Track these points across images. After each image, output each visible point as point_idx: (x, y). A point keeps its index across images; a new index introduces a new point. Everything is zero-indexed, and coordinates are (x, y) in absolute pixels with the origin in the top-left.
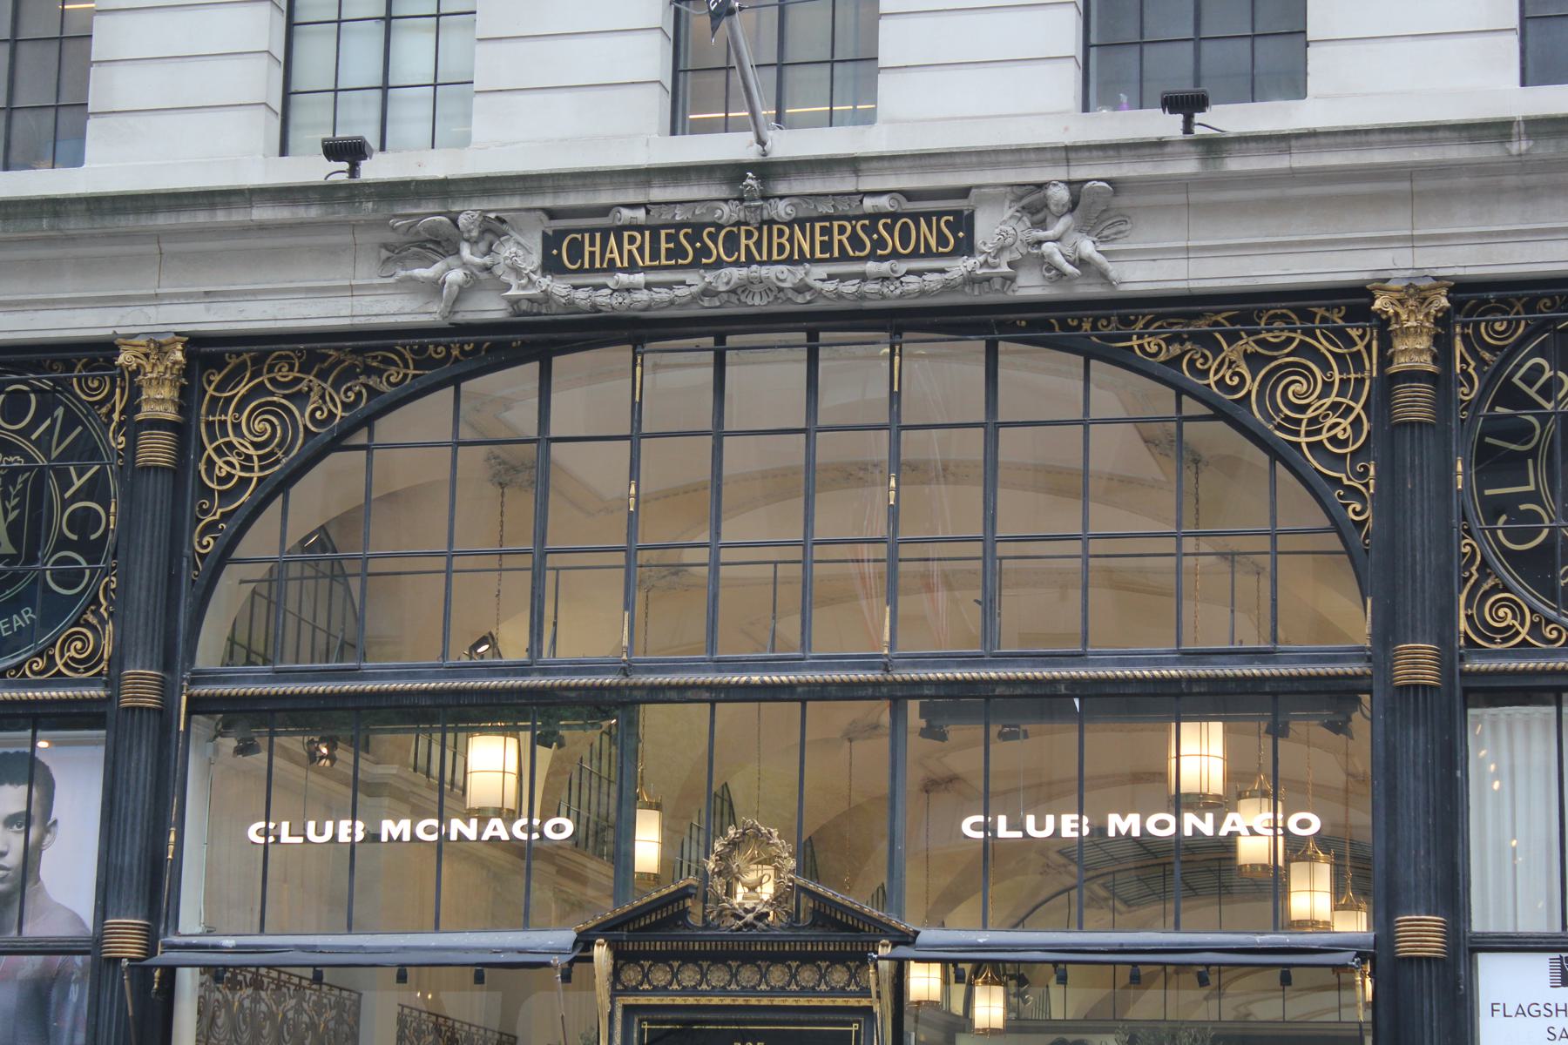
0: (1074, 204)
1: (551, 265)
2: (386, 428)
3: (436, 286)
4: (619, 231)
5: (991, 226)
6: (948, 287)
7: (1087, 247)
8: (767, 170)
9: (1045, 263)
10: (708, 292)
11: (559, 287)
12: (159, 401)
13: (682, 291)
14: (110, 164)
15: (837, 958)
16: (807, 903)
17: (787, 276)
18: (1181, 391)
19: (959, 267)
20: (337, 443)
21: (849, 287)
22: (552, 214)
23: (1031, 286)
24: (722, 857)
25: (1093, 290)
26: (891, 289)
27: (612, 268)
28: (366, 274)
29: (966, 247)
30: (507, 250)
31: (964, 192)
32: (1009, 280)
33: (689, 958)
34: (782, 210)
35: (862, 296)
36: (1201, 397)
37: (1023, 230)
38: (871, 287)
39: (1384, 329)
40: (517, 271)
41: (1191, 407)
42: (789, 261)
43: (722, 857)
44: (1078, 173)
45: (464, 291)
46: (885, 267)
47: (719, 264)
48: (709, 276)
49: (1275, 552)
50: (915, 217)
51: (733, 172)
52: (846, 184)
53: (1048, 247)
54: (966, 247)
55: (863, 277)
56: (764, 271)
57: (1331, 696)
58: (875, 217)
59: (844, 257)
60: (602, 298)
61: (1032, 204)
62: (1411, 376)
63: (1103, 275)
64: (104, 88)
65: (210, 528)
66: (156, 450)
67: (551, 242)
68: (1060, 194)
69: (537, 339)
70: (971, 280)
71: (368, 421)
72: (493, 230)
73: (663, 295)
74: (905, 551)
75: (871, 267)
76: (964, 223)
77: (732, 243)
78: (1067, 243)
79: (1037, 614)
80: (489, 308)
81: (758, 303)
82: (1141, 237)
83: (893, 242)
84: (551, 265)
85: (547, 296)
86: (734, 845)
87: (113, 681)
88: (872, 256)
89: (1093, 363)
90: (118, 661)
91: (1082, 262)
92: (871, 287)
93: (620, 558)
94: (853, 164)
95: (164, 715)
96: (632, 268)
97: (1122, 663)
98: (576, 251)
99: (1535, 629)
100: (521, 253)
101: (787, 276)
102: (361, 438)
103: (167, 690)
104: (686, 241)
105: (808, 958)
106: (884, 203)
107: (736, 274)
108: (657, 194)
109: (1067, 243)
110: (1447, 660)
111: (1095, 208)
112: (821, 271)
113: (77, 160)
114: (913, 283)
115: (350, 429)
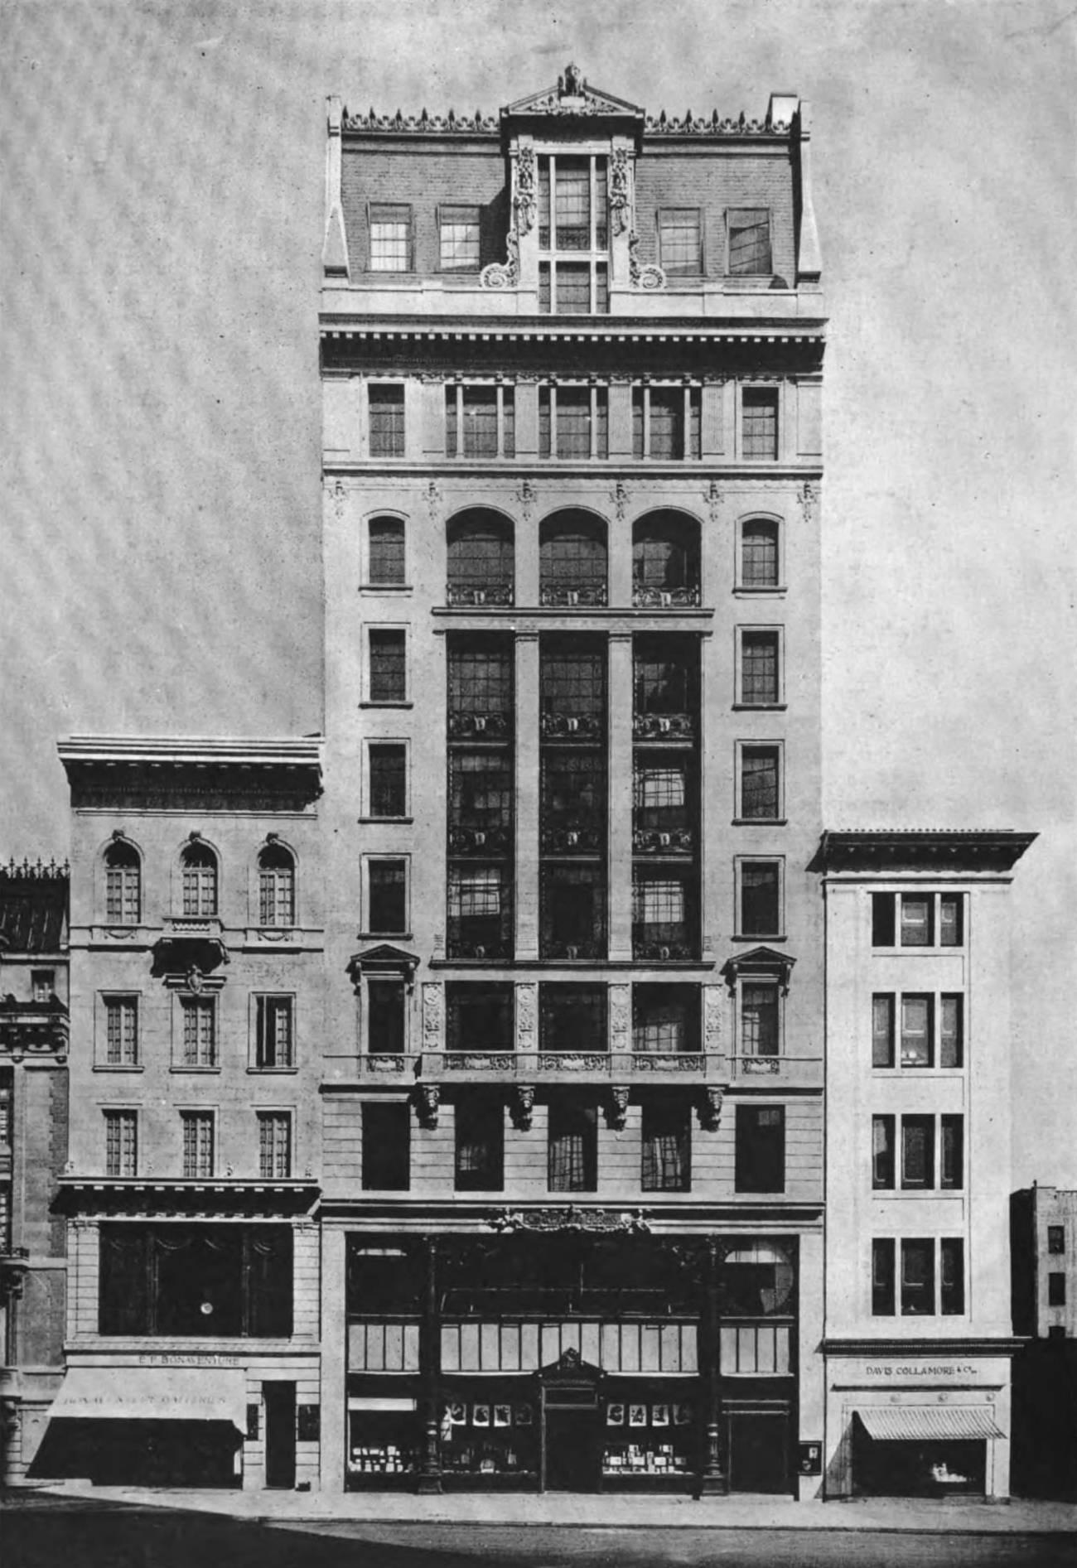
61: (635, 1213)
72: (512, 1212)
109: (640, 1221)
113: (404, 1185)
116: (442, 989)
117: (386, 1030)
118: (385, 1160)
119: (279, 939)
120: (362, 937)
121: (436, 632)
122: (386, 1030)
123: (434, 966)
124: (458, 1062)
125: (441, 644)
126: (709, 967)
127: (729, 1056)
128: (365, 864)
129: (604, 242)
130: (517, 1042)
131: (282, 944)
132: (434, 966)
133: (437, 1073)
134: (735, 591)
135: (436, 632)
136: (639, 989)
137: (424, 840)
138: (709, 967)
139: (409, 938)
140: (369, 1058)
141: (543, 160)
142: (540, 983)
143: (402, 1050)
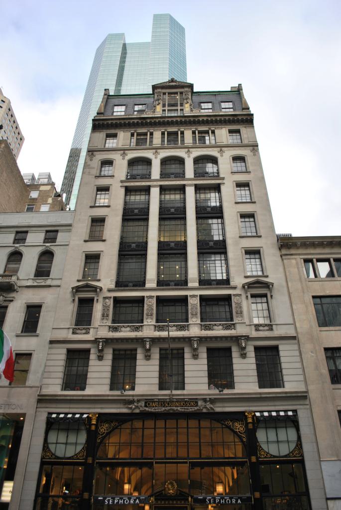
0: (210, 401)
1: (146, 406)
2: (123, 426)
3: (131, 408)
4: (154, 402)
5: (200, 403)
6: (195, 410)
7: (212, 406)
8: (173, 395)
9: (206, 408)
10: (165, 410)
11: (147, 409)
12: (94, 422)
13: (162, 410)
14: (89, 391)
15: (182, 500)
16: (179, 492)
17: (175, 408)
18: (222, 424)
19: (196, 408)
20: (116, 428)
21: (183, 410)
22: (146, 399)
23: (205, 410)
24: (167, 485)
25: (212, 411)
26: (188, 410)
27: (153, 407)
28: (122, 406)
29: (197, 406)
30: (140, 404)
31: (197, 399)
32: (202, 410)
33: (163, 500)
34: (175, 400)
35: (184, 411)
36: (225, 425)
37: (204, 404)
38: (186, 410)
39: (246, 416)
40: (141, 406)
41: (224, 426)
42: (175, 407)
43: (167, 485)
44: (210, 397)
45: (135, 409)
46: (187, 408)
47: (167, 407)
48: (166, 408)
49: (235, 445)
50: (191, 401)
51: (169, 395)
52: (183, 397)
53: (207, 406)
54: (197, 406)
55: (185, 409)
56: (173, 408)
57: (242, 464)
58: (186, 401)
59: (182, 406)
60: (152, 410)
62: (250, 423)
63: (213, 410)
64: (89, 381)
65: (100, 438)
66: (93, 428)
67: (146, 403)
68: (208, 399)
69: (144, 416)
70: (198, 410)
71: (120, 425)
73: (160, 410)
74: (190, 444)
75: (186, 408)
76: (197, 403)
77: (168, 404)
78: (209, 405)
79: (207, 451)
80: (137, 411)
81: (171, 411)
82: (218, 405)
83: (188, 405)
84: (146, 406)
85: (145, 410)
86: (169, 484)
87: (86, 459)
88: (186, 406)
89: (212, 421)
90: (87, 456)
91: (211, 408)
92: (186, 410)
93: (164, 444)
94: (184, 395)
95: (93, 463)
96: (156, 407)
97: (217, 459)
98: (149, 404)
99: (267, 455)
100: (143, 404)
101: (175, 408)
102: (119, 427)
103: (93, 461)
104: (162, 403)
105: (179, 500)
106: (187, 400)
107: (170, 408)
108: (159, 398)
110: (257, 458)
111: (213, 401)
112: (179, 408)
114: (191, 410)
115: (118, 426)
116: (112, 300)
117: (83, 318)
118: (75, 377)
119: (41, 282)
120: (78, 281)
121: (121, 187)
122: (83, 318)
123: (109, 291)
124: (115, 329)
125: (123, 191)
126: (235, 288)
127: (247, 323)
128: (84, 255)
129: (182, 105)
130: (145, 320)
131: (43, 284)
132: (109, 291)
133: (104, 333)
134: (232, 173)
135: (121, 187)
136: (203, 299)
137: (109, 249)
138: (235, 288)
139: (99, 280)
140: (74, 329)
141: (164, 94)
142: (156, 296)
143: (90, 326)
